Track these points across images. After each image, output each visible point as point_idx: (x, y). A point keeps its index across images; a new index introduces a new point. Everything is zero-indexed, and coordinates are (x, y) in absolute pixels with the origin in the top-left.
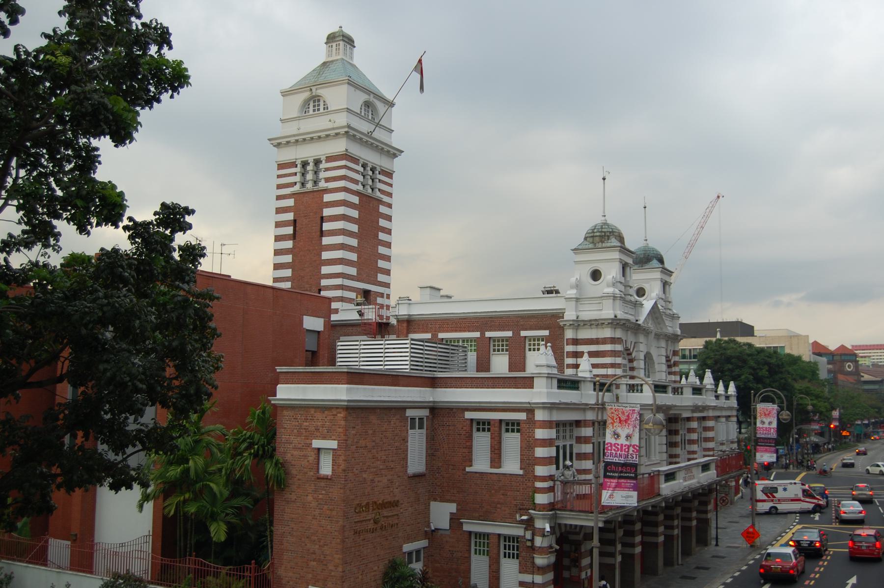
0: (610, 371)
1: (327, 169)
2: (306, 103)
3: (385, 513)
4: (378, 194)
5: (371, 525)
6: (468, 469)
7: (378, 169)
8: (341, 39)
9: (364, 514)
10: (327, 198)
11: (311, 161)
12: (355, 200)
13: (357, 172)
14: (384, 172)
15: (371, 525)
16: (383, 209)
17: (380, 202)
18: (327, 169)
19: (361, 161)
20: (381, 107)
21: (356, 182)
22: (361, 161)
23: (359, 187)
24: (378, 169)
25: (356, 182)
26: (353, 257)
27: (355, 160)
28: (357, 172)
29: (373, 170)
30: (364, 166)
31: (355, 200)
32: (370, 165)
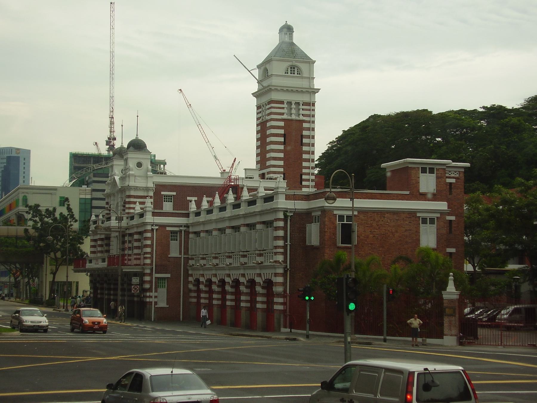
1: (268, 109)
4: (301, 118)
7: (301, 103)
8: (287, 29)
10: (268, 124)
12: (282, 124)
13: (283, 108)
14: (305, 104)
16: (305, 125)
18: (268, 109)
20: (304, 67)
21: (282, 114)
22: (285, 102)
23: (285, 117)
24: (301, 103)
25: (282, 114)
26: (281, 155)
27: (282, 102)
28: (283, 108)
31: (282, 124)
32: (293, 103)
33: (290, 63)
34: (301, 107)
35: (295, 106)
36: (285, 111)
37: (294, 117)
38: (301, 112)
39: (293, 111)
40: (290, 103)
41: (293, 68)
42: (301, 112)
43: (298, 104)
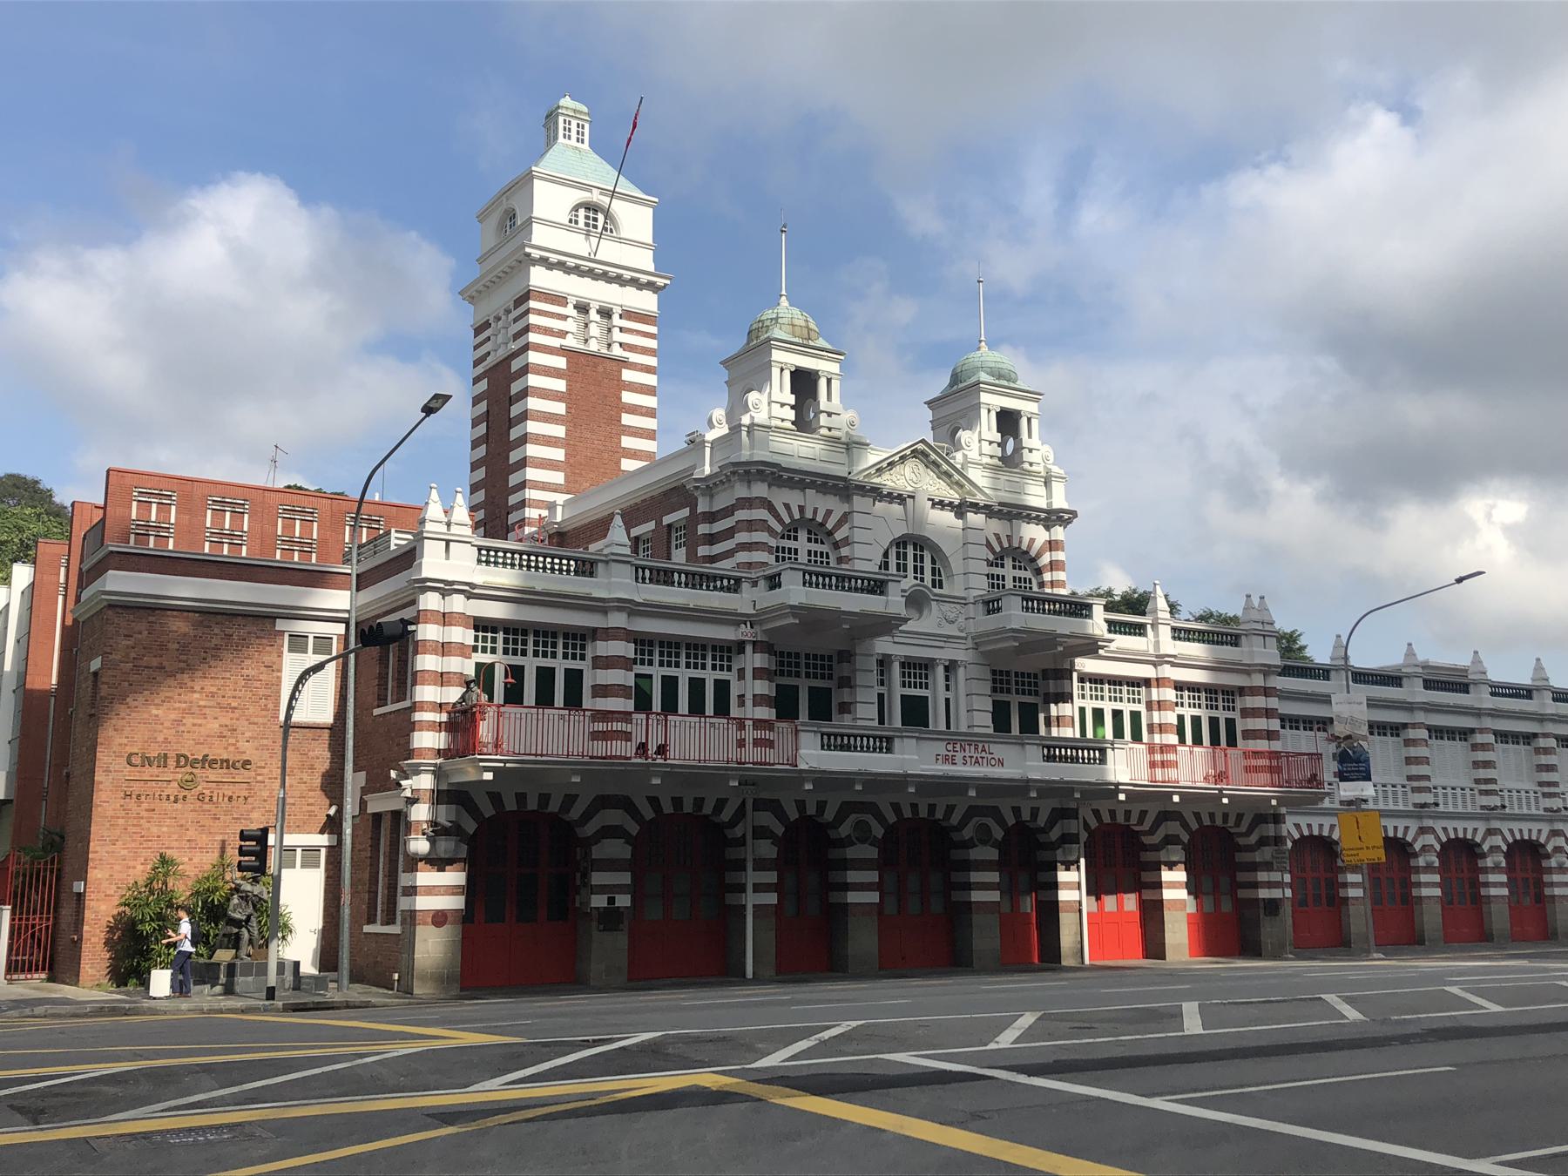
0: (742, 557)
2: (501, 226)
3: (213, 775)
4: (617, 351)
5: (173, 789)
6: (376, 712)
7: (617, 311)
9: (154, 770)
11: (501, 313)
12: (560, 362)
13: (564, 318)
14: (628, 314)
15: (173, 789)
16: (628, 375)
17: (625, 363)
19: (572, 301)
22: (572, 301)
23: (571, 342)
24: (617, 311)
25: (563, 334)
27: (560, 300)
28: (564, 318)
29: (606, 313)
30: (583, 308)
31: (560, 362)
32: (594, 307)
33: (582, 196)
34: (616, 320)
35: (597, 318)
36: (569, 325)
37: (593, 346)
38: (617, 336)
39: (594, 330)
40: (583, 308)
41: (591, 207)
42: (617, 336)
43: (606, 313)
